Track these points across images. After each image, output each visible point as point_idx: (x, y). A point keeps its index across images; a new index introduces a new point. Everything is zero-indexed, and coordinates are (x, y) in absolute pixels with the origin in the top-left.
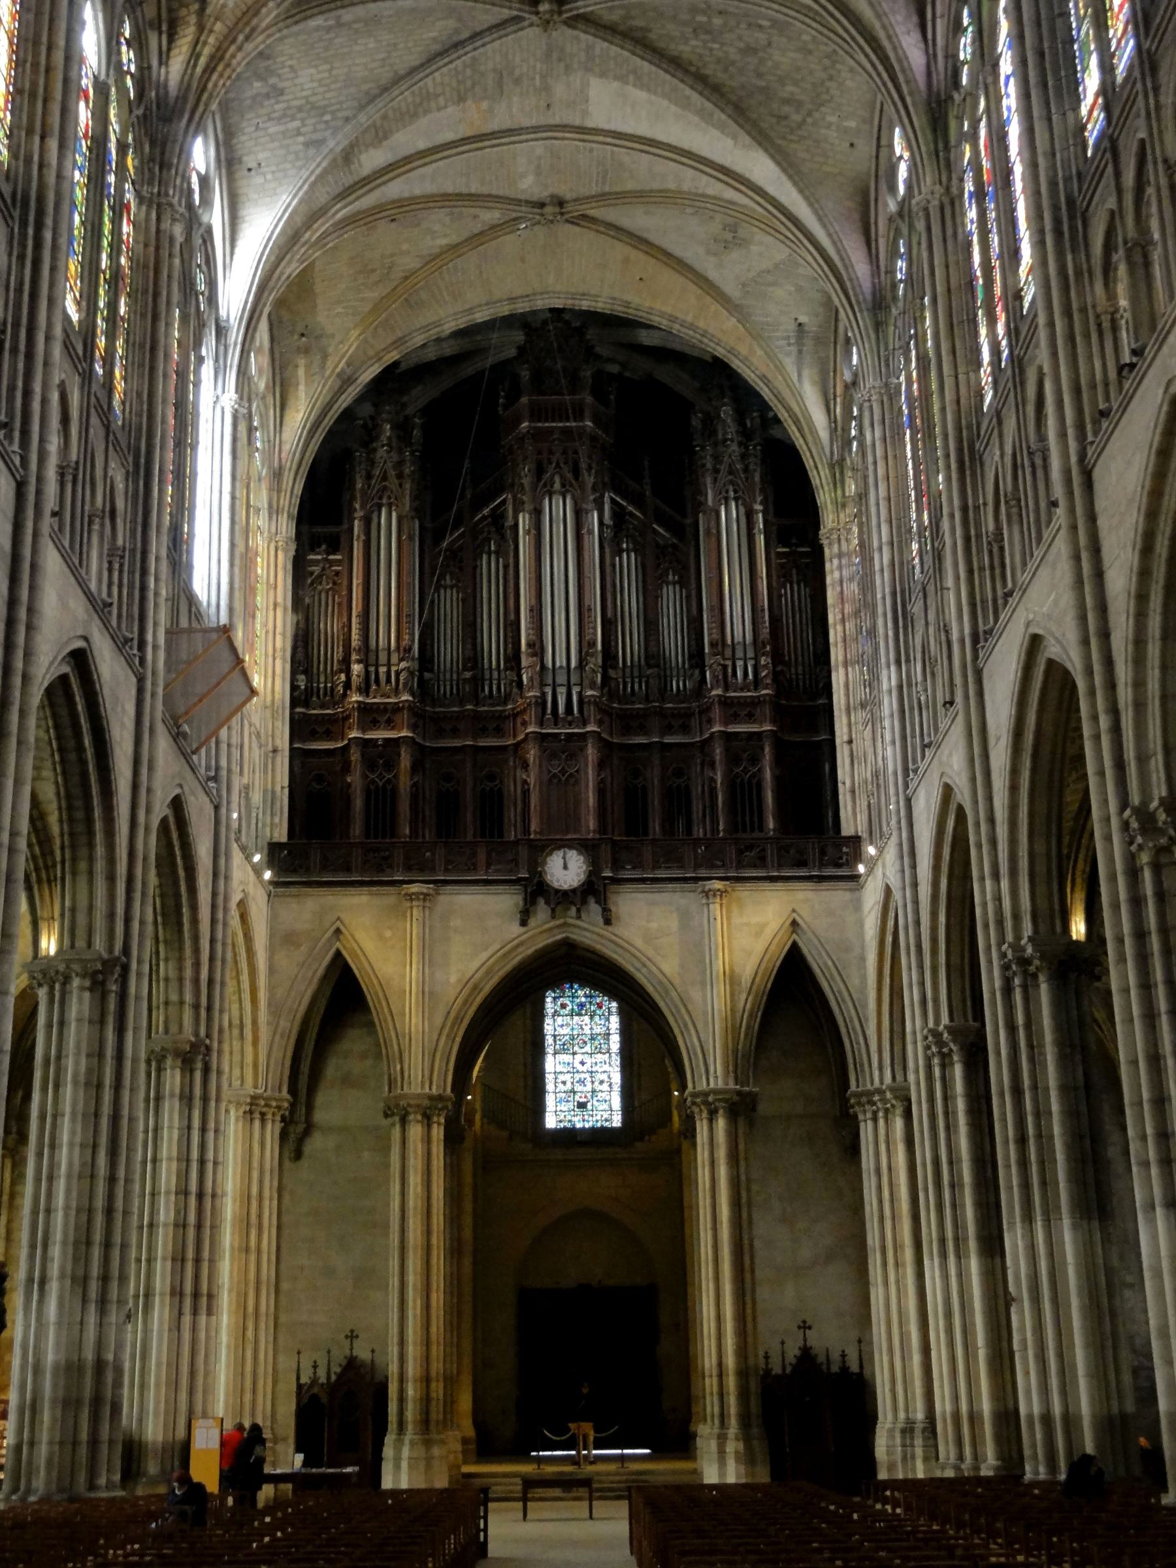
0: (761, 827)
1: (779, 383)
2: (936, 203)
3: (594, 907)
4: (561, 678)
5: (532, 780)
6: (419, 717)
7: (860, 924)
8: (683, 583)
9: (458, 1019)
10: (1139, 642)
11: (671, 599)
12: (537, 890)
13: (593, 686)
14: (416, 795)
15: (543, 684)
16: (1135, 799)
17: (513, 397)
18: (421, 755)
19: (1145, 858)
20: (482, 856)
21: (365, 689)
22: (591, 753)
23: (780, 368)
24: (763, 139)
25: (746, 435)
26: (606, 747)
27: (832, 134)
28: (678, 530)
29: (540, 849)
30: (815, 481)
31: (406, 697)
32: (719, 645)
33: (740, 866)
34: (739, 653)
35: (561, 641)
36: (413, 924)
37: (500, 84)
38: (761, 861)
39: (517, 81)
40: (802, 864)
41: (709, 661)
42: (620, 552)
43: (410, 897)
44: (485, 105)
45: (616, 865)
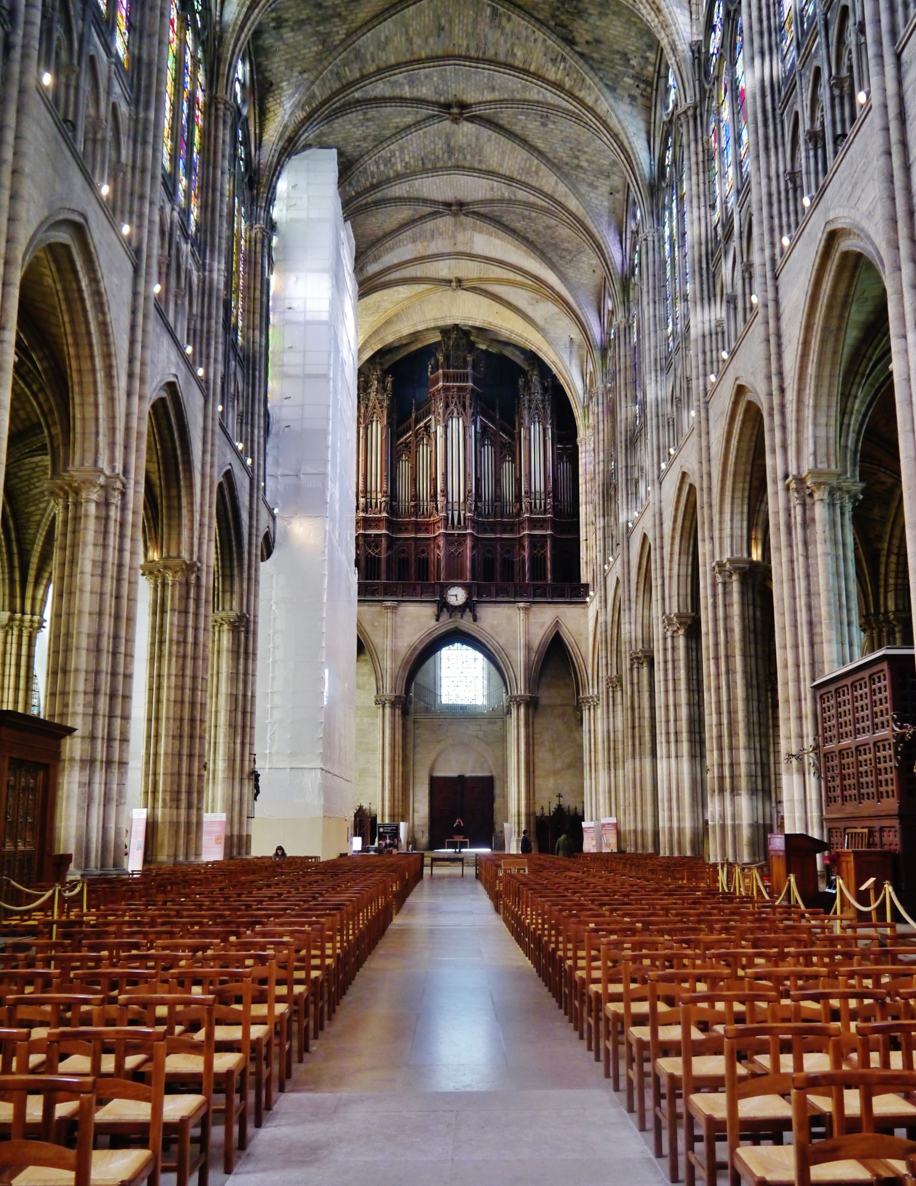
0: (545, 578)
1: (560, 365)
2: (622, 326)
3: (468, 615)
4: (456, 507)
5: (442, 554)
6: (391, 525)
7: (587, 623)
8: (513, 461)
9: (407, 662)
10: (672, 554)
11: (507, 467)
12: (443, 606)
13: (470, 511)
14: (388, 559)
15: (447, 510)
16: (667, 612)
17: (436, 368)
18: (391, 541)
19: (669, 634)
20: (419, 589)
21: (365, 510)
22: (469, 542)
23: (561, 359)
24: (553, 266)
25: (545, 390)
26: (475, 539)
27: (585, 266)
28: (512, 436)
29: (445, 588)
30: (576, 414)
31: (384, 514)
32: (529, 492)
33: (535, 596)
34: (538, 496)
35: (457, 487)
36: (388, 619)
37: (433, 236)
38: (543, 595)
39: (441, 234)
40: (562, 596)
41: (524, 500)
42: (484, 445)
43: (387, 608)
44: (425, 244)
45: (479, 595)
